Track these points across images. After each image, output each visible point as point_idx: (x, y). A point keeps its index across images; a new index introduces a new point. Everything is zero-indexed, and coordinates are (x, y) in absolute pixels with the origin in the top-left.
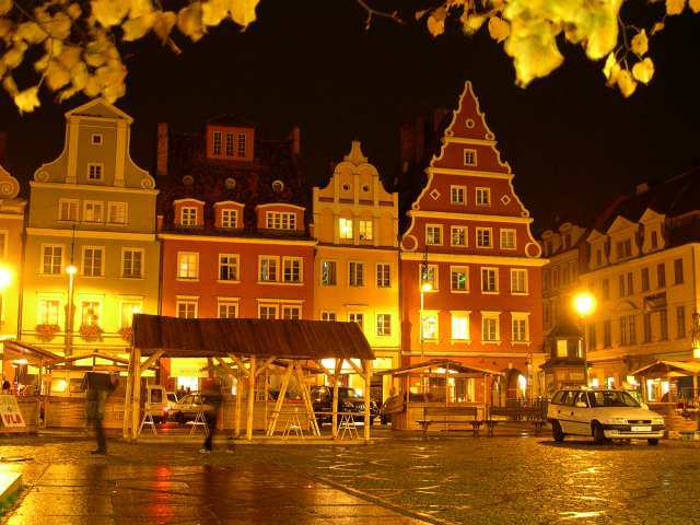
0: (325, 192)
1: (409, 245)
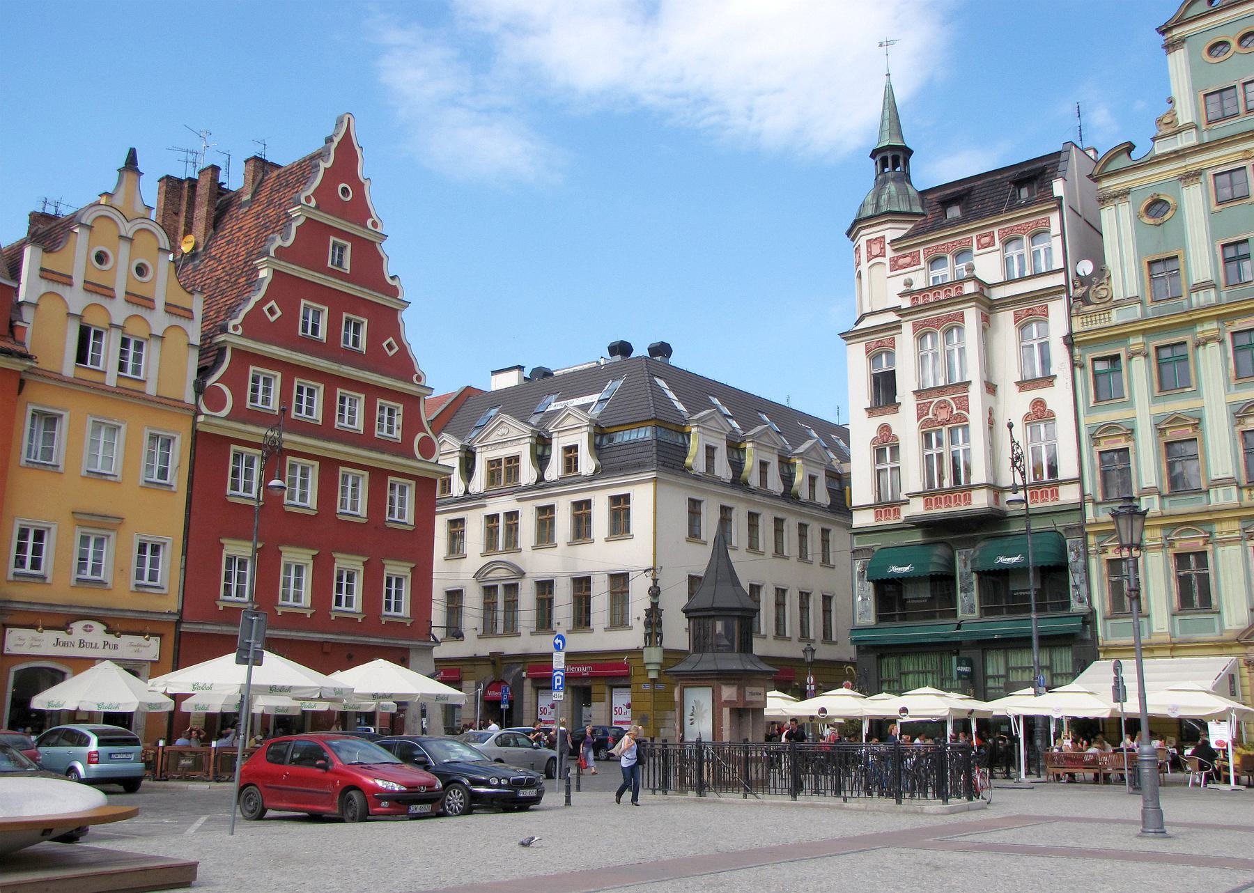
0: (53, 262)
1: (216, 401)
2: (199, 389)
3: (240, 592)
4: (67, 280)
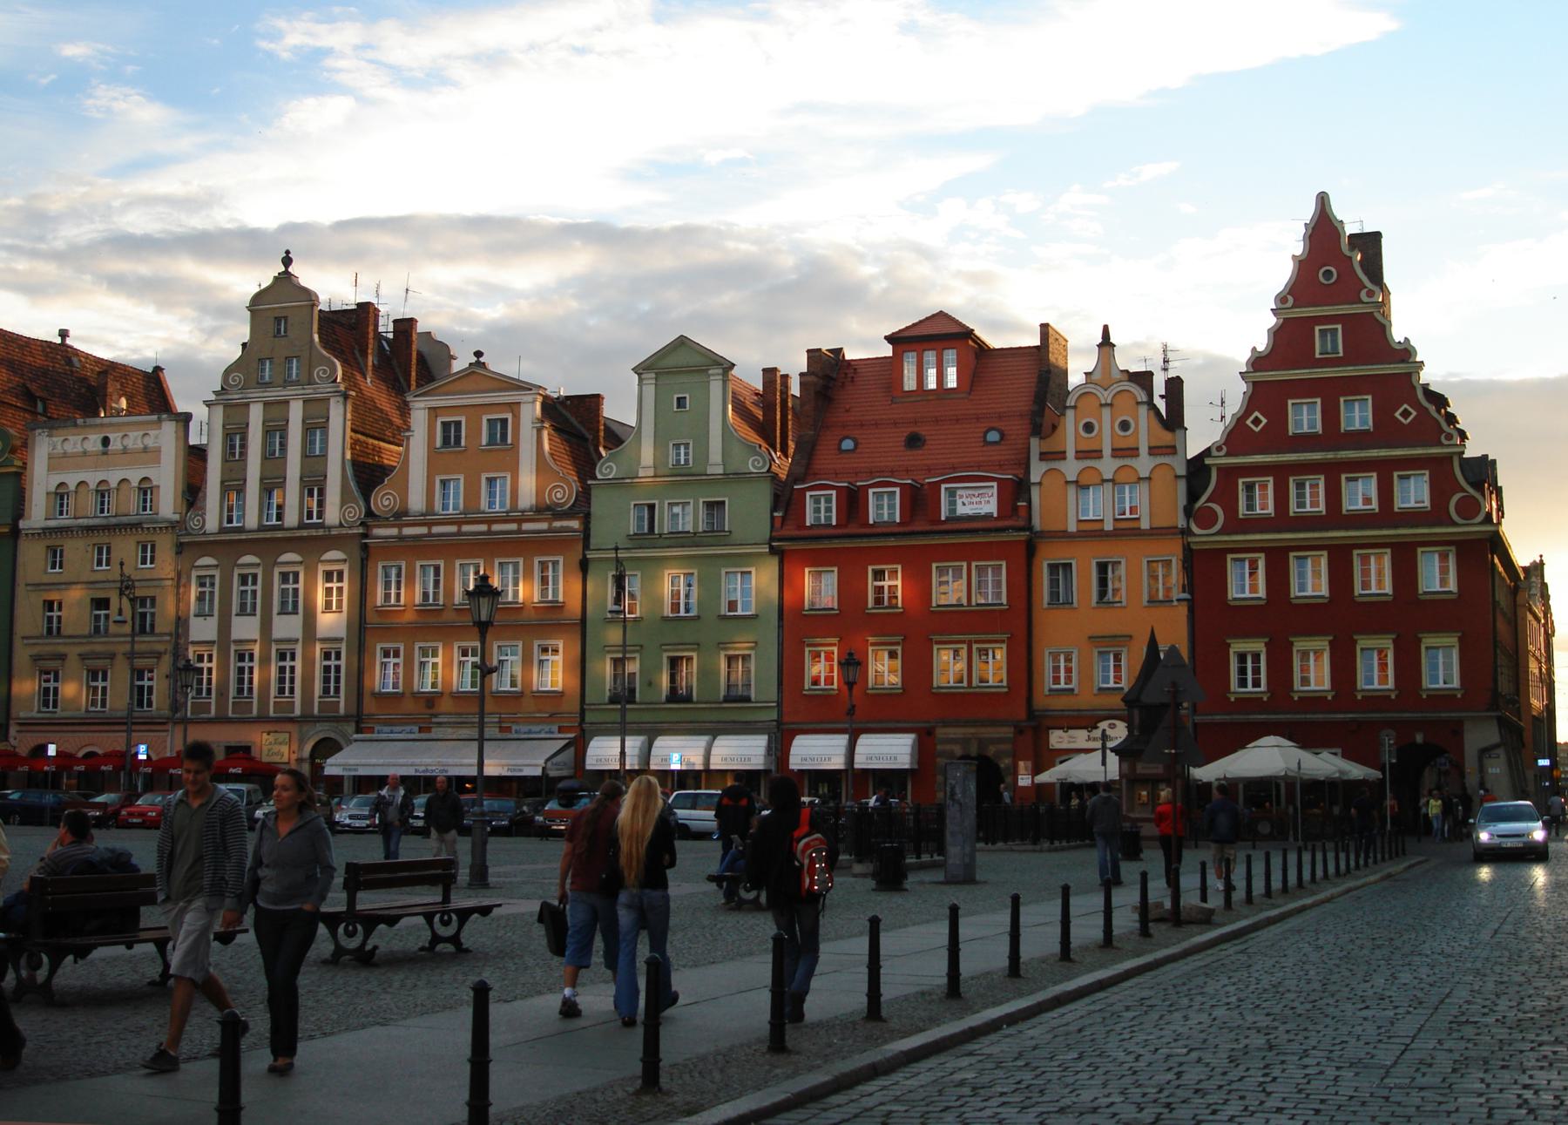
1: (1207, 519)
2: (1188, 512)
3: (1256, 683)
4: (1061, 456)
